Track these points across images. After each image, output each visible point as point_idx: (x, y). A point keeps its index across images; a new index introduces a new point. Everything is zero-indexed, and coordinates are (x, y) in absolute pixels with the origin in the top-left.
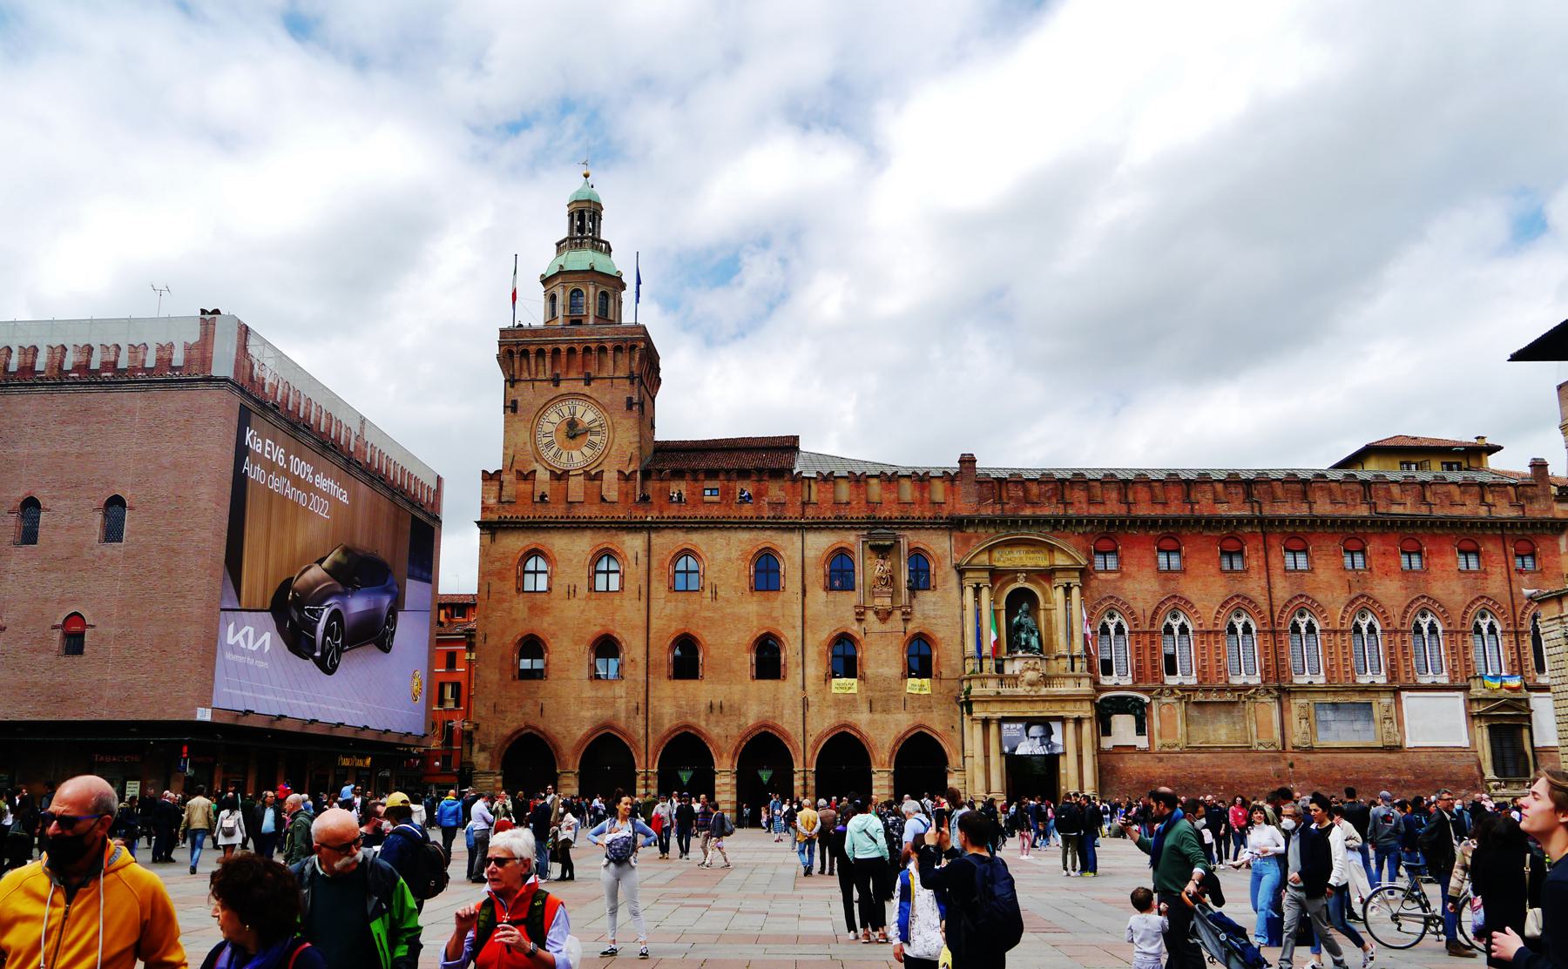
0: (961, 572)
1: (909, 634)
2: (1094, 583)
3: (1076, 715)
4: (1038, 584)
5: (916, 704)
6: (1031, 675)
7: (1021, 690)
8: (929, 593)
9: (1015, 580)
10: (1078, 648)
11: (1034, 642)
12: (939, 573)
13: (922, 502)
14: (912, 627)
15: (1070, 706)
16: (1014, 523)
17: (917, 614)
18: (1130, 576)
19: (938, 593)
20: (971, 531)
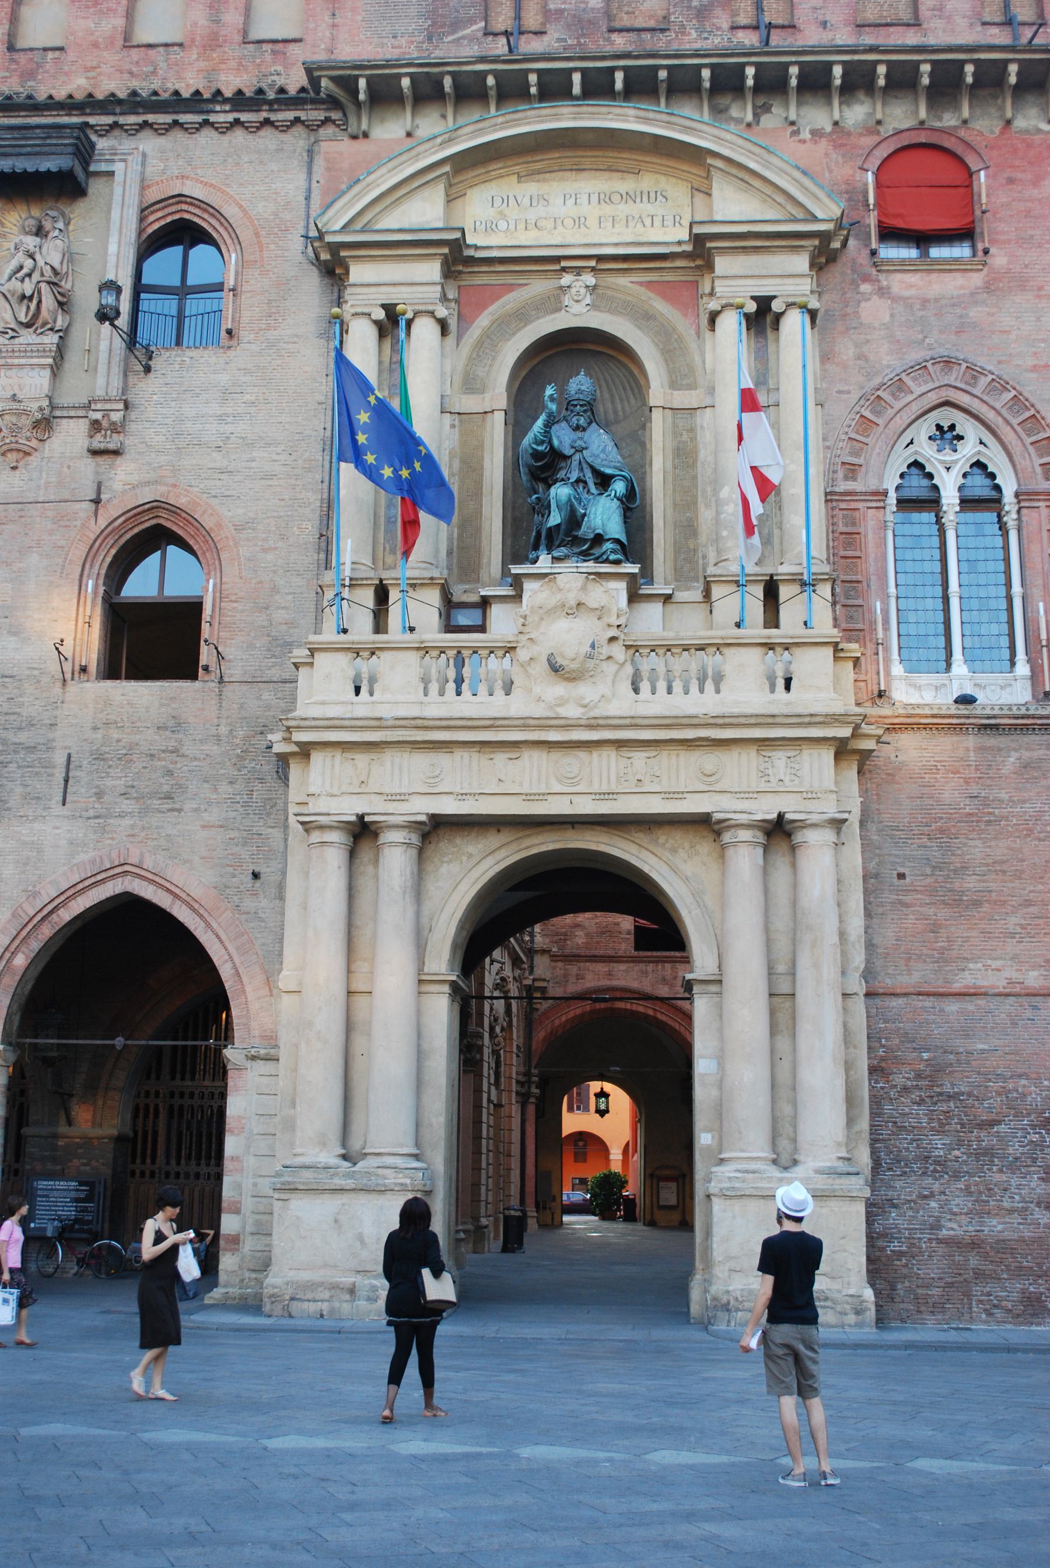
0: (333, 267)
1: (112, 510)
2: (874, 311)
3: (766, 810)
4: (645, 318)
5: (116, 781)
6: (568, 636)
7: (536, 698)
8: (208, 357)
9: (553, 303)
10: (804, 538)
11: (604, 515)
12: (254, 282)
13: (213, 42)
14: (129, 483)
15: (739, 769)
16: (554, 88)
17: (149, 434)
18: (1021, 283)
19: (242, 355)
20: (389, 129)
